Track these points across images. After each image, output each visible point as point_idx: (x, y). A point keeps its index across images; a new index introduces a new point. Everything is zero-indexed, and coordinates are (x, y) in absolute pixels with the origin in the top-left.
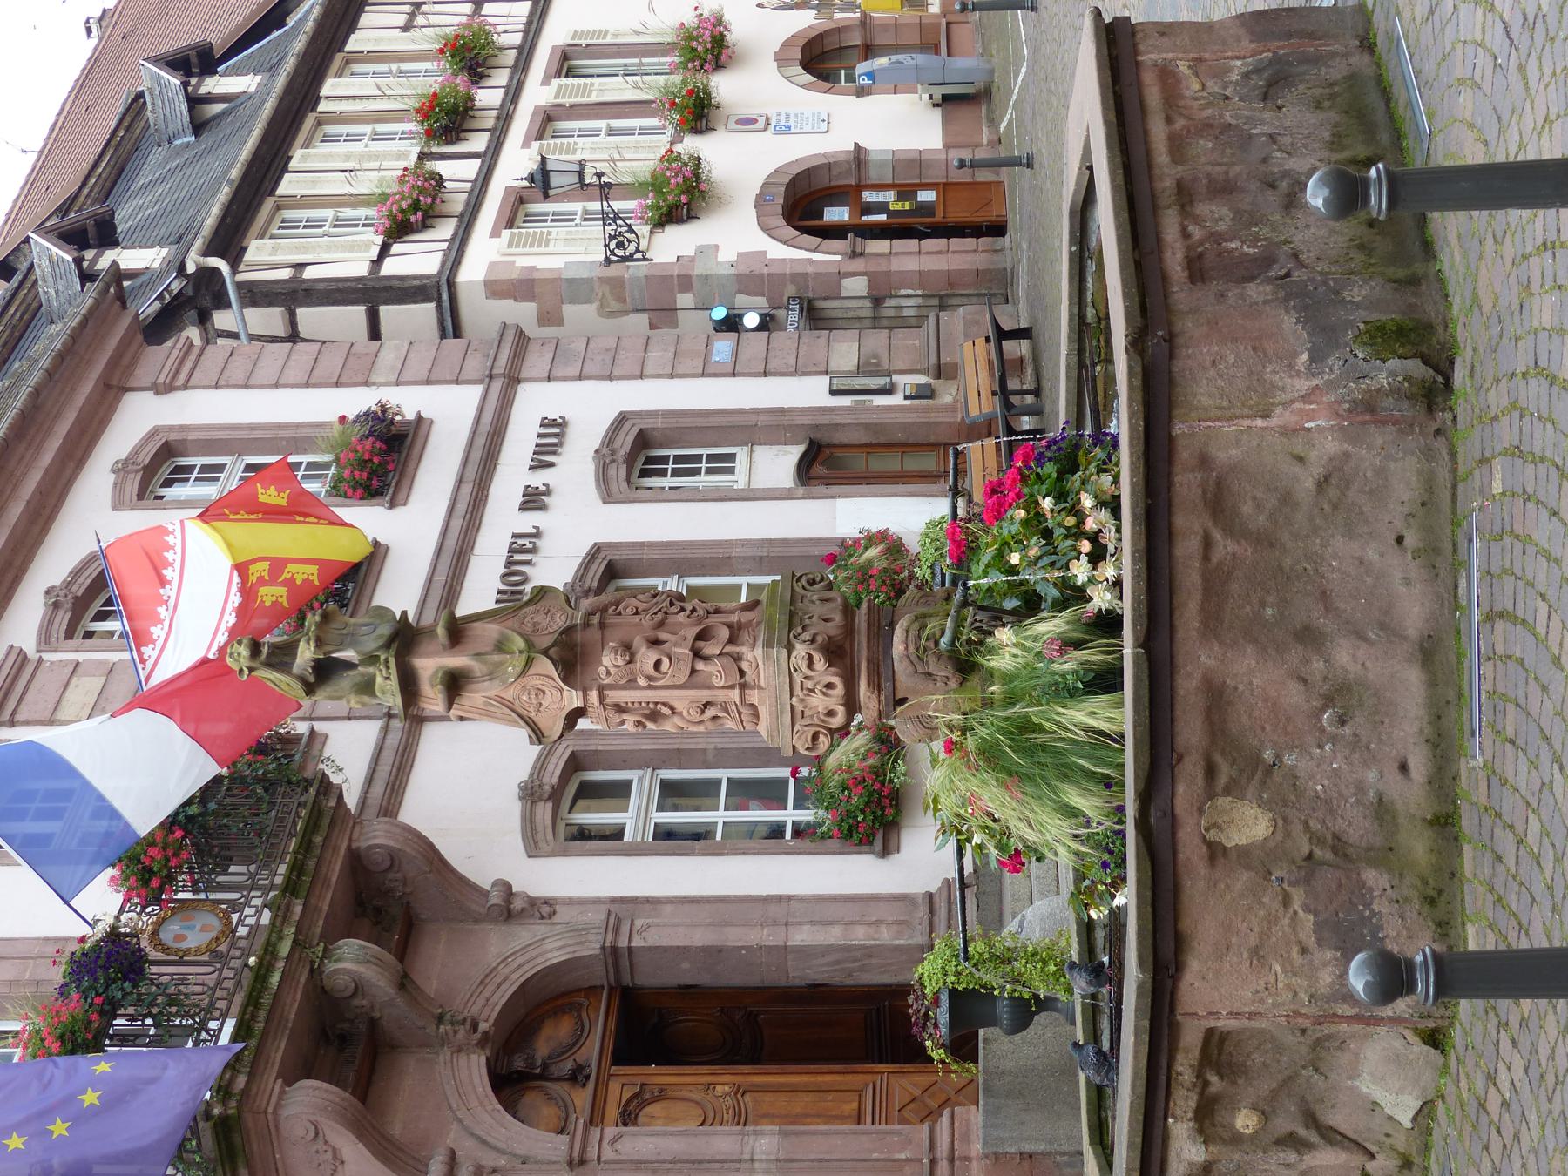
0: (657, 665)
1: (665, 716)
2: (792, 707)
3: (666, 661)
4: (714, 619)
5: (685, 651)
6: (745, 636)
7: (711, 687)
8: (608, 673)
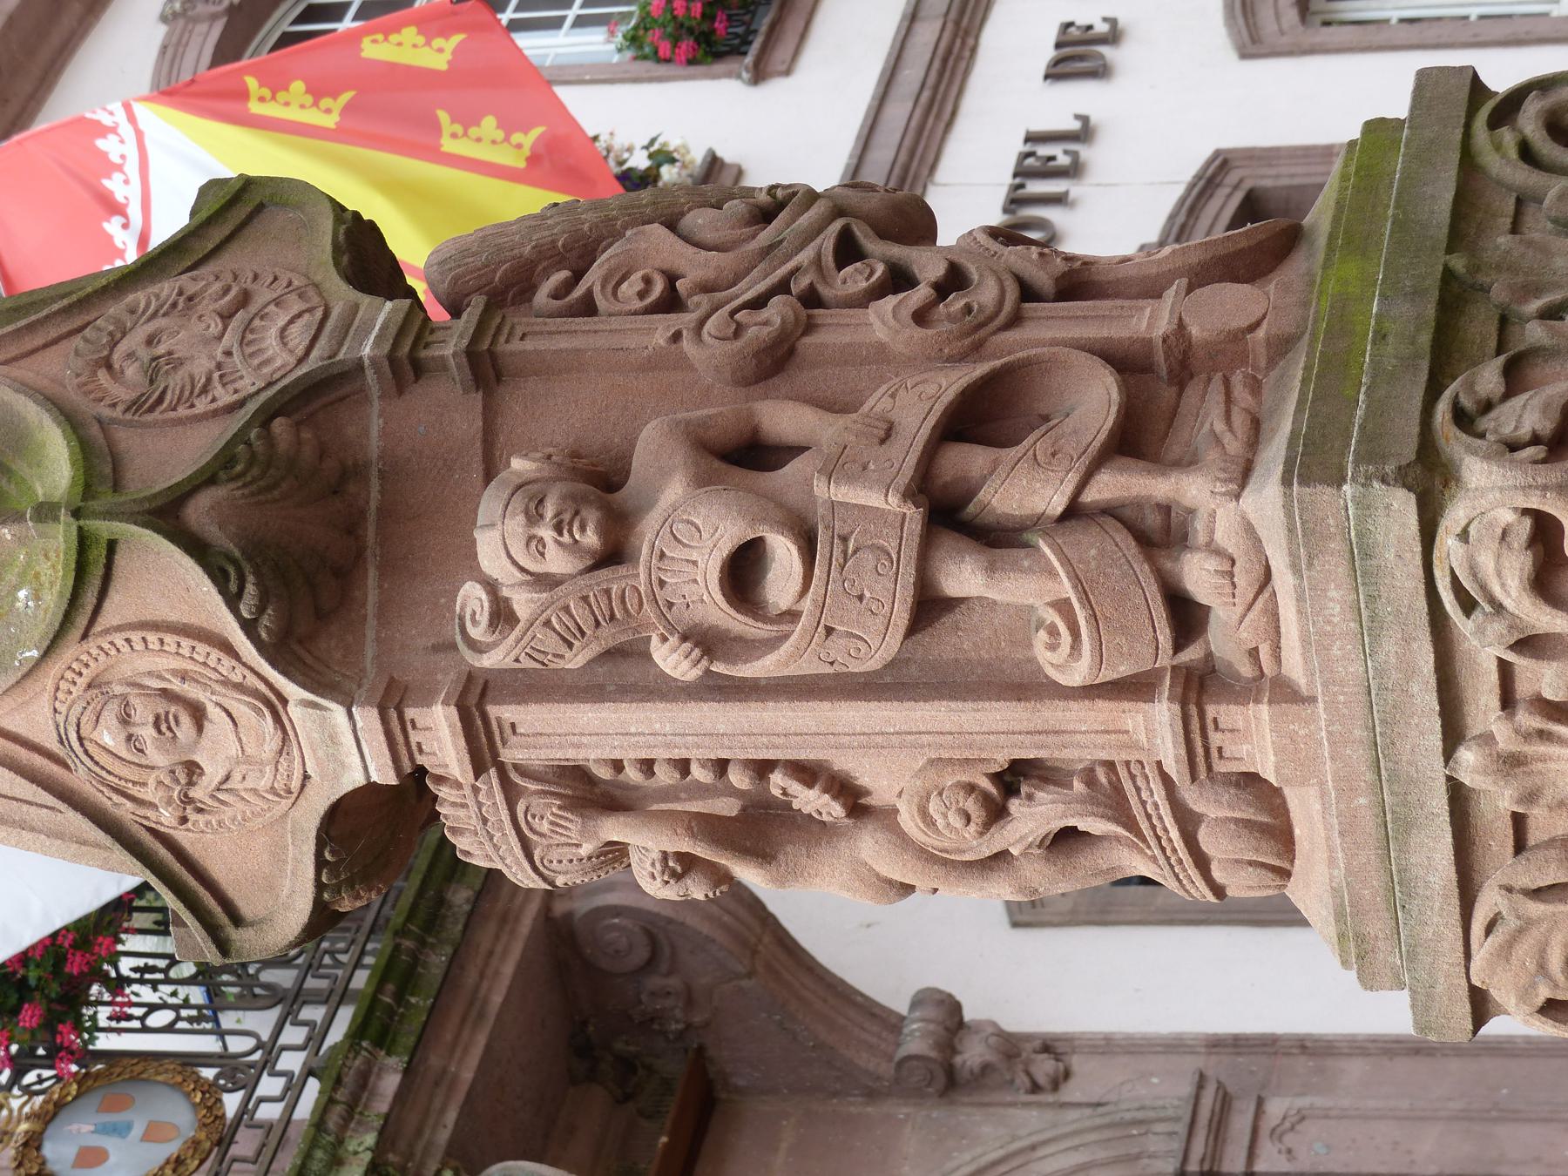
0: (743, 572)
1: (813, 830)
2: (1458, 796)
3: (783, 552)
4: (1050, 328)
5: (877, 501)
6: (1208, 417)
7: (1028, 687)
8: (502, 615)
